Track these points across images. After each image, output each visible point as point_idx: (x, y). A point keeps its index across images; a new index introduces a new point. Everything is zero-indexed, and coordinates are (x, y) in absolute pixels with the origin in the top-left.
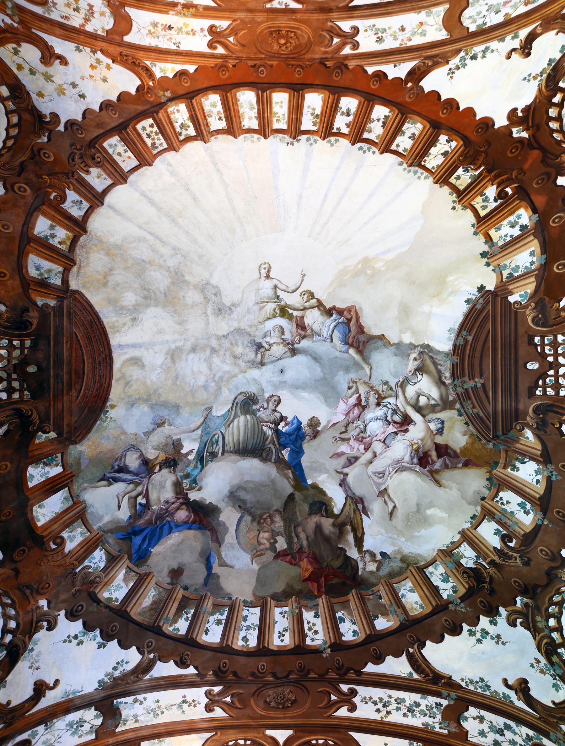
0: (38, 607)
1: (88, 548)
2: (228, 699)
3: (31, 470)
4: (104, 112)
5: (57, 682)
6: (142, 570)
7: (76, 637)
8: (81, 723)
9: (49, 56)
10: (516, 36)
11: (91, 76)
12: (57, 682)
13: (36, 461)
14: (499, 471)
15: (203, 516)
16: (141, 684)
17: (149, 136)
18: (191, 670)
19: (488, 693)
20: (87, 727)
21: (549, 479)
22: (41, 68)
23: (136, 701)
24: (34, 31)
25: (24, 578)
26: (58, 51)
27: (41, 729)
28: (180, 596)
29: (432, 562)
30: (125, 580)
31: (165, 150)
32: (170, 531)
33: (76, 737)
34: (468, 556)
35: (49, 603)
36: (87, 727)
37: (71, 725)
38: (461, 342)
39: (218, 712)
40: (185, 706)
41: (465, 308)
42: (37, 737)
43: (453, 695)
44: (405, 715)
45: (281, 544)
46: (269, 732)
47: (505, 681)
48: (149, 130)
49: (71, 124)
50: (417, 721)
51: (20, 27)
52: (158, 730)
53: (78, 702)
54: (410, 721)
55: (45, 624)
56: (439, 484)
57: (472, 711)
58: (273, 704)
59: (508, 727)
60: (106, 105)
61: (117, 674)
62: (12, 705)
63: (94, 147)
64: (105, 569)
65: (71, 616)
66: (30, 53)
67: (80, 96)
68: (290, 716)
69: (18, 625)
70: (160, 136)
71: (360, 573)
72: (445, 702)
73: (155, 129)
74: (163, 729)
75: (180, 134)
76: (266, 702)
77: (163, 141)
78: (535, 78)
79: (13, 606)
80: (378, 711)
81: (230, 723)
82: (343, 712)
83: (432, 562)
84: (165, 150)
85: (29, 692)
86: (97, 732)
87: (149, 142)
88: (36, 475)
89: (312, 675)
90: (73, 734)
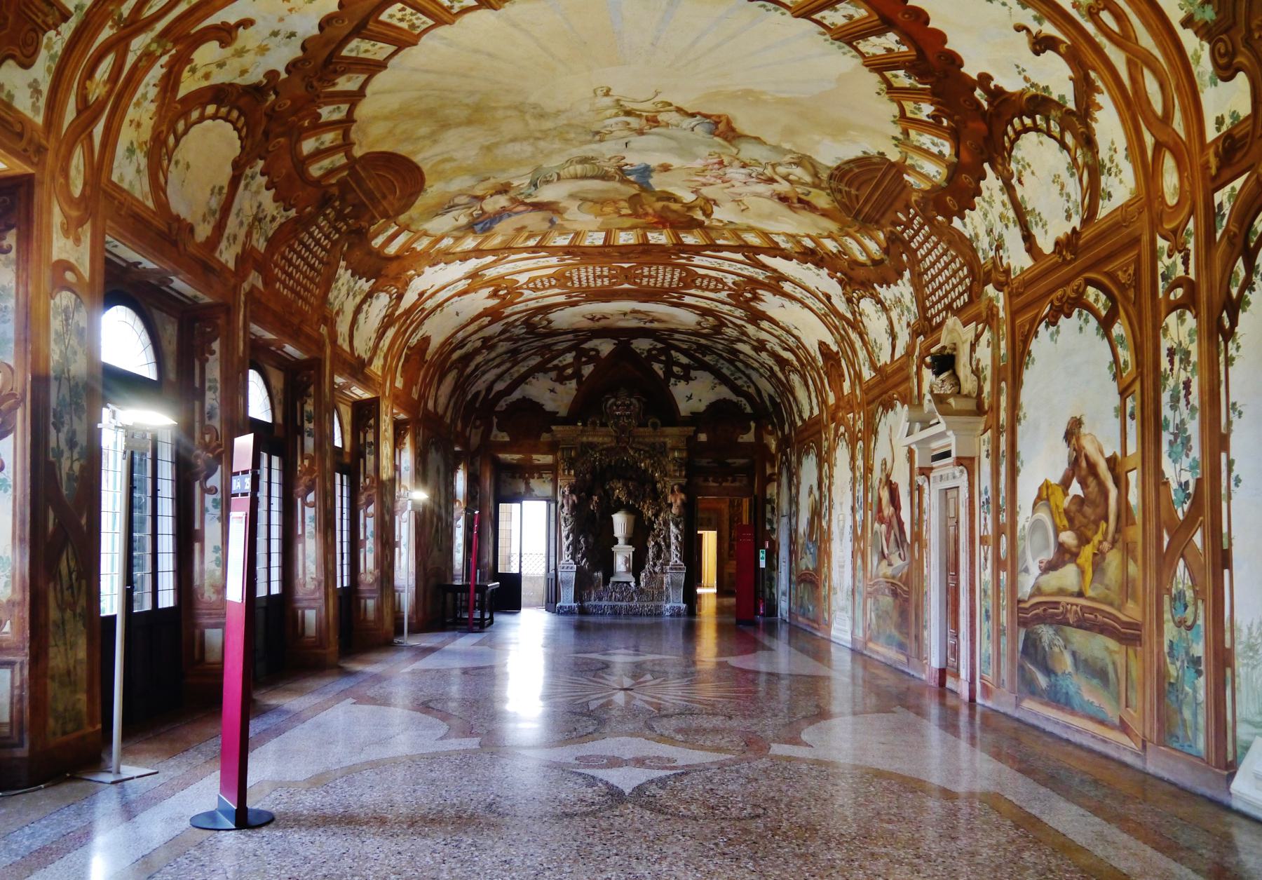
3: (373, 243)
4: (327, 30)
9: (225, 34)
10: (1039, 20)
11: (290, 10)
13: (376, 236)
14: (851, 231)
17: (401, 20)
22: (229, 51)
24: (193, 31)
25: (392, 274)
26: (232, 21)
31: (432, 27)
34: (809, 243)
38: (847, 167)
41: (860, 154)
48: (399, 15)
49: (292, 67)
51: (179, 47)
60: (325, 23)
63: (331, 63)
66: (207, 53)
67: (289, 37)
70: (420, 15)
73: (409, 10)
75: (452, 7)
77: (425, 18)
78: (1026, 79)
84: (432, 27)
87: (404, 25)
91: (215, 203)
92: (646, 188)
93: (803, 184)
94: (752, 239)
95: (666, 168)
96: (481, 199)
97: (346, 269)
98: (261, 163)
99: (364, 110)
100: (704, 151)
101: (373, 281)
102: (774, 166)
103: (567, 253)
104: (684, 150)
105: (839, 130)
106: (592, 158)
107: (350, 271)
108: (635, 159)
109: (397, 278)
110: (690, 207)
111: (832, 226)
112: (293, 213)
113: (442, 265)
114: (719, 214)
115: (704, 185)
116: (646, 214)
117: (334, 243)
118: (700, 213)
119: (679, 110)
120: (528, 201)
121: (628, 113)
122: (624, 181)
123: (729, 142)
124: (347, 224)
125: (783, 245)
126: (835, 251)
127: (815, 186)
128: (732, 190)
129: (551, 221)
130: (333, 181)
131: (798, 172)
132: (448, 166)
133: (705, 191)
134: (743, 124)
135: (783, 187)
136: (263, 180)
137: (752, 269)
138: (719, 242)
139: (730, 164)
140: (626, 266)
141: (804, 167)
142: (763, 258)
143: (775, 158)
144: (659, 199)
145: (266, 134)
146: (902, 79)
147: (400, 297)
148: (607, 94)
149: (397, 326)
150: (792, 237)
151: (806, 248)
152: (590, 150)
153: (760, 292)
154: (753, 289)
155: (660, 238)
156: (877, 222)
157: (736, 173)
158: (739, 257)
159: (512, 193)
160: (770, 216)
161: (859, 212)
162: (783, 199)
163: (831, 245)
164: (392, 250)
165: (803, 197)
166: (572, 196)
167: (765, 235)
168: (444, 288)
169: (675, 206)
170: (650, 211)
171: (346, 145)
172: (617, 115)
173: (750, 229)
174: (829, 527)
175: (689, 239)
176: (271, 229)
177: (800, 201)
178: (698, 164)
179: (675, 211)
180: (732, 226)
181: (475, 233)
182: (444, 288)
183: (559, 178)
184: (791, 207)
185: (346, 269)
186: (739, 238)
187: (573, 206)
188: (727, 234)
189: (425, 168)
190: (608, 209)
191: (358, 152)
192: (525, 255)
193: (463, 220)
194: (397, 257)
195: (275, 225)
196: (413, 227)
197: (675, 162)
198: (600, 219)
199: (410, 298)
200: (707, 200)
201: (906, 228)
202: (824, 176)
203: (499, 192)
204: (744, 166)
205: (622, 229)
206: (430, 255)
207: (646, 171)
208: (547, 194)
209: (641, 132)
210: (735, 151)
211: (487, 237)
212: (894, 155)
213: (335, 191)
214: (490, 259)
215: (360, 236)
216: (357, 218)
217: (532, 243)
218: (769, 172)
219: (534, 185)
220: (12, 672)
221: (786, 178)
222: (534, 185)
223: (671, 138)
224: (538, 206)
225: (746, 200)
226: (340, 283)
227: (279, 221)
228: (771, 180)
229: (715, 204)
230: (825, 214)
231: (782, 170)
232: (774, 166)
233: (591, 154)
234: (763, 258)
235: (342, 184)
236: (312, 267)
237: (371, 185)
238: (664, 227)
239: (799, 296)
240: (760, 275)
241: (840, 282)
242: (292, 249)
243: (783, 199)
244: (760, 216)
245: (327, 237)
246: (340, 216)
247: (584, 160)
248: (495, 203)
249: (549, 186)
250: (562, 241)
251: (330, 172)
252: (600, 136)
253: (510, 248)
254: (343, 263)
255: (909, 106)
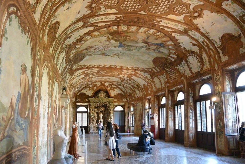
0: (184, 51)
1: (171, 49)
2: (154, 21)
3: (173, 61)
5: (191, 42)
6: (163, 42)
7: (182, 44)
8: (193, 34)
12: (191, 42)
13: (171, 60)
15: (145, 42)
16: (175, 30)
18: (161, 28)
19: (77, 31)
20: (192, 33)
21: (69, 58)
23: (179, 29)
27: (199, 41)
28: (157, 37)
29: (90, 39)
30: (167, 43)
32: (154, 43)
33: (196, 33)
34: (82, 42)
35: (183, 50)
36: (192, 33)
37: (195, 36)
39: (159, 20)
40: (167, 23)
42: (201, 41)
43: (86, 26)
44: (101, 18)
45: (128, 37)
46: (146, 14)
47: (73, 35)
50: (96, 18)
52: (178, 22)
53: (190, 37)
54: (98, 17)
55: (185, 49)
56: (88, 46)
57: (81, 26)
58: (142, 19)
59: (73, 30)
61: (179, 34)
62: (198, 49)
64: (170, 46)
65: (181, 46)
68: (138, 16)
69: (188, 53)
71: (109, 34)
72: (89, 23)
74: (176, 22)
76: (143, 20)
79: (187, 55)
80: (108, 17)
81: (156, 17)
82: (119, 16)
83: (90, 39)
85: (195, 46)
86: (191, 30)
88: (173, 60)
89: (127, 22)
90: (196, 34)
91: (160, 83)
92: (121, 43)
93: (89, 52)
94: (96, 33)
95: (115, 47)
96: (154, 50)
97: (177, 66)
98: (158, 76)
99: (147, 67)
100: (107, 51)
101: (183, 60)
102: (95, 52)
103: (155, 25)
104: (111, 50)
105: (87, 60)
106: (128, 51)
107: (178, 66)
108: (120, 49)
109: (185, 54)
110: (112, 39)
111: (80, 50)
112: (165, 74)
113: (180, 44)
114: (105, 38)
115: (108, 44)
116: (124, 36)
117: (171, 68)
118: (110, 38)
119: (110, 56)
120: (147, 45)
121: (118, 56)
122: (125, 44)
123: (103, 53)
124: (168, 66)
125: (88, 36)
126: (76, 47)
127: (87, 53)
128: (102, 45)
129: (148, 38)
130: (160, 68)
131: (90, 53)
132: (150, 57)
133: (108, 43)
134: (101, 56)
135: (92, 49)
136: (160, 76)
137: (95, 21)
138: (106, 29)
139: (103, 50)
140: (142, 12)
141: (89, 54)
142: (92, 28)
143: (95, 53)
144: (119, 40)
145: (155, 75)
146: (83, 66)
147: (192, 52)
148: (120, 58)
149: (204, 53)
150: (86, 41)
151: (82, 41)
152: (128, 52)
153: (90, 12)
154: (92, 11)
155: (124, 28)
156: (74, 58)
157: (102, 48)
158: (99, 25)
159: (148, 47)
160: (93, 42)
161: (77, 55)
162: (91, 47)
163: (78, 47)
164: (175, 57)
165: (88, 50)
166: (138, 43)
167: (93, 37)
168: (193, 38)
169: (116, 39)
170: (122, 37)
171: (153, 68)
172: (120, 56)
173: (97, 36)
174: (38, 109)
175: (115, 28)
176: (166, 78)
177: (88, 49)
178: (109, 48)
179: (116, 37)
180: (102, 35)
181: (164, 45)
182: (193, 38)
183: (137, 47)
184: (89, 47)
185: (177, 66)
186: (100, 32)
187: (140, 41)
188: (103, 32)
189: (153, 59)
190: (132, 38)
191: (155, 66)
192: (166, 29)
193: (162, 48)
194: (178, 55)
195: (166, 76)
196: (168, 54)
197: (113, 48)
198: (136, 36)
199: (196, 49)
200: (108, 41)
201: (71, 63)
202: (86, 55)
203: (150, 49)
204: (100, 50)
205: (133, 32)
206: (176, 49)
207: (119, 46)
208: (143, 45)
209: (117, 53)
210: (102, 52)
211: (164, 42)
212: (78, 63)
213: (162, 68)
214: (174, 34)
215: (171, 63)
216: (167, 64)
217: (159, 33)
218: (95, 51)
219: (142, 47)
220: (233, 147)
221: (92, 51)
222: (142, 47)
223: (113, 52)
224: (146, 42)
225: (99, 43)
226: (180, 68)
227: (165, 76)
228: (95, 50)
229: (106, 41)
230: (83, 50)
231: (93, 52)
232: (95, 52)
233: (128, 51)
234: (92, 28)
235: (160, 67)
236: (174, 73)
237: (160, 63)
238: (121, 32)
239: (76, 25)
240: (92, 20)
241: (71, 44)
242: (169, 76)
243: (91, 47)
244: (95, 41)
245: (170, 69)
246: (167, 67)
247: (130, 50)
248: (153, 47)
249: (140, 46)
250: (152, 31)
251: (159, 68)
252: (124, 54)
253: (165, 35)
254: (176, 67)
255: (80, 66)
